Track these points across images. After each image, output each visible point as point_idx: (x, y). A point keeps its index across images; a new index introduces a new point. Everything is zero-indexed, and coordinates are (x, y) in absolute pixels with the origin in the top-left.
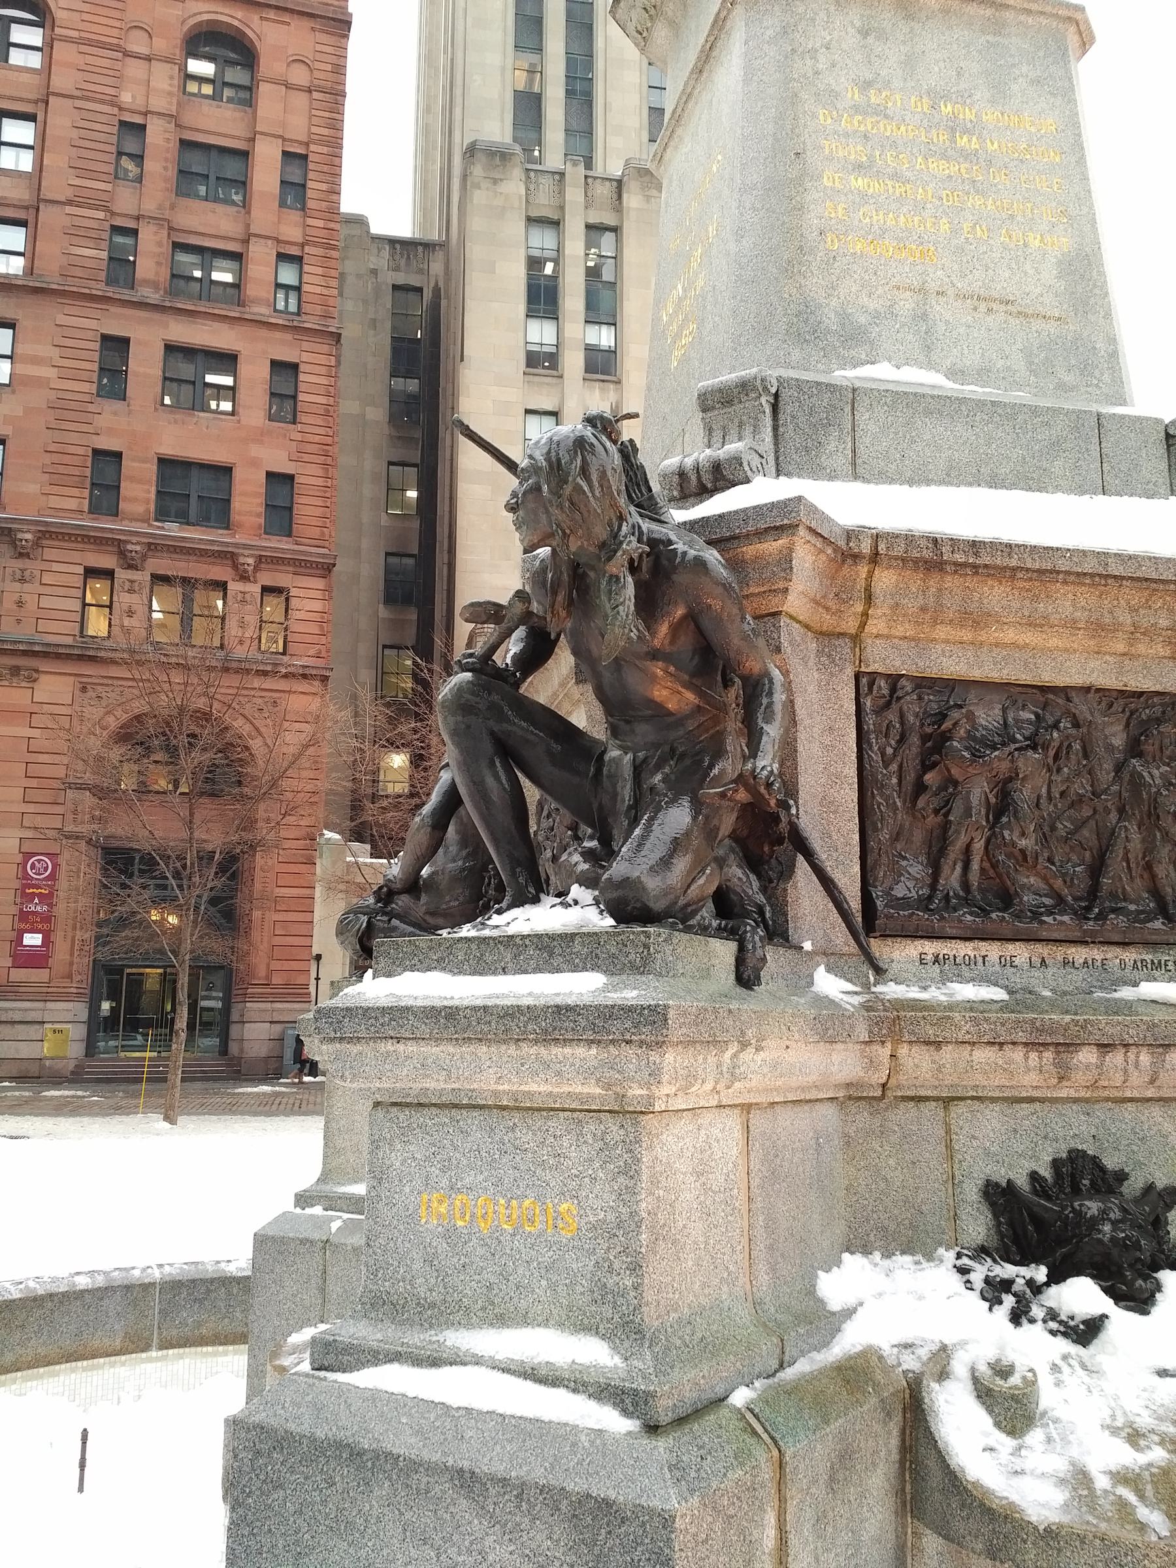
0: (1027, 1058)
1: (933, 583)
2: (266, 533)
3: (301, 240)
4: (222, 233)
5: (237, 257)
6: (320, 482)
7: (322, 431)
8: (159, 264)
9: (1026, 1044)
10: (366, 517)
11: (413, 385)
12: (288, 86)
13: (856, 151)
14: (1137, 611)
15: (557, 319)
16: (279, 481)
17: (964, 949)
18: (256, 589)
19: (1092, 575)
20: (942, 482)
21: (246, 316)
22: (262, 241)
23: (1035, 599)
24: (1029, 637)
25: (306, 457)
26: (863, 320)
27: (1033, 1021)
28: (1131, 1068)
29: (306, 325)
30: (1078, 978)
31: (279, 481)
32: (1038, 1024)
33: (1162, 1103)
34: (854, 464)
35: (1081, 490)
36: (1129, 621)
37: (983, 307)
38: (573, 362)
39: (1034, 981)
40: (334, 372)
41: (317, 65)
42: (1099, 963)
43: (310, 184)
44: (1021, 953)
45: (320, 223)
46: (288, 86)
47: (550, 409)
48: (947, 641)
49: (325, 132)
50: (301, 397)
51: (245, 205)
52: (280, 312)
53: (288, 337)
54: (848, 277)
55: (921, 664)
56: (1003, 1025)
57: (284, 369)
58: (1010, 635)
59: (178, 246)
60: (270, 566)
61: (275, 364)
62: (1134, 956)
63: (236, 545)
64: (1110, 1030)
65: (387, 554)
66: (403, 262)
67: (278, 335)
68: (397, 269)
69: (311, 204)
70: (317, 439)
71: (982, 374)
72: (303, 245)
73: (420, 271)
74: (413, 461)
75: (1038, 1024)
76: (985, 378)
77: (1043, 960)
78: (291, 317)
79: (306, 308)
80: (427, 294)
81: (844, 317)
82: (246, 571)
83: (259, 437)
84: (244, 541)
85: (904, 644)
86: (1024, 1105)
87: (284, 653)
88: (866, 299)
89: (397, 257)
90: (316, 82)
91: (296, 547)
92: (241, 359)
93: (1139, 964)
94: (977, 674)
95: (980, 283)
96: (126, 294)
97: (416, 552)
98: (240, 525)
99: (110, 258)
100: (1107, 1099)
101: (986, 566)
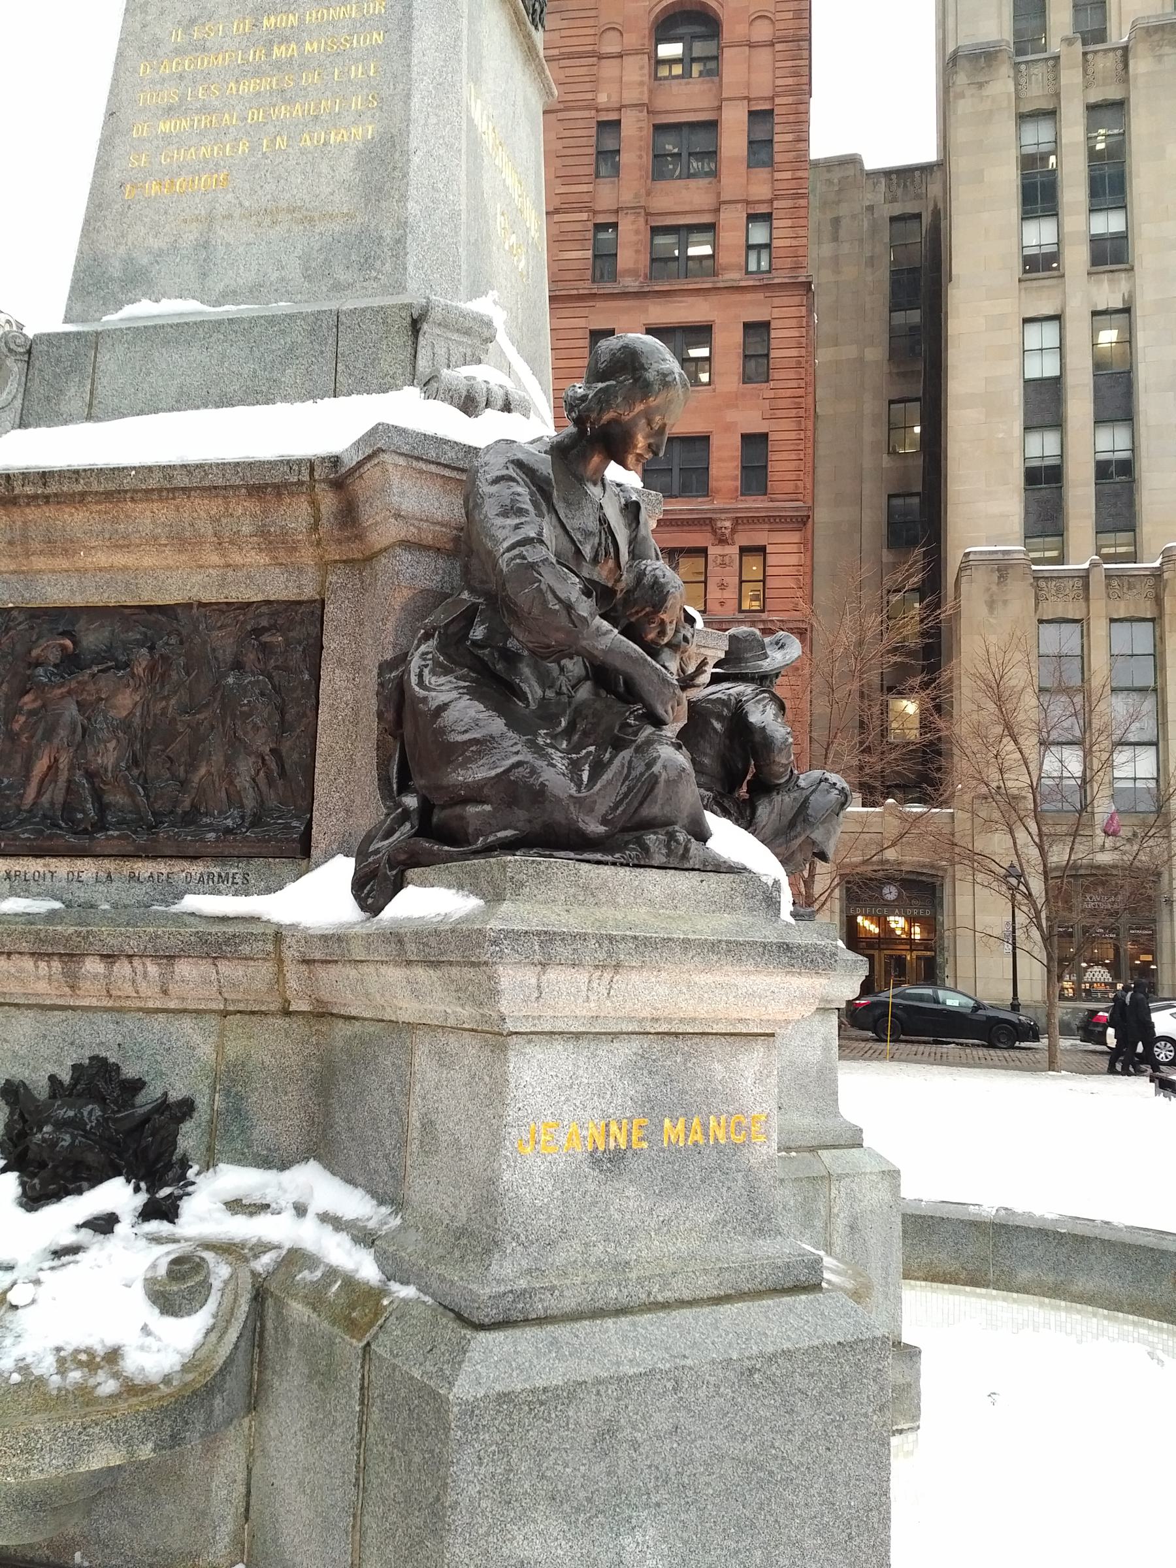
0: (37, 967)
1: (16, 513)
2: (742, 495)
3: (769, 196)
4: (697, 208)
5: (710, 228)
6: (793, 435)
7: (794, 384)
8: (637, 251)
9: (33, 954)
10: (868, 462)
11: (915, 317)
12: (751, 45)
13: (170, 95)
14: (219, 520)
15: (1125, 207)
16: (754, 443)
17: (33, 866)
18: (733, 550)
19: (160, 490)
20: (172, 409)
21: (719, 285)
22: (733, 206)
23: (115, 520)
24: (120, 559)
25: (779, 413)
26: (145, 261)
27: (38, 933)
28: (139, 978)
29: (776, 281)
30: (139, 892)
31: (754, 443)
32: (42, 935)
33: (194, 1015)
34: (90, 405)
35: (312, 395)
36: (210, 532)
37: (267, 221)
38: (1077, 257)
39: (97, 896)
40: (805, 323)
41: (779, 16)
42: (164, 877)
43: (776, 138)
44: (88, 868)
45: (788, 175)
46: (751, 45)
47: (1052, 313)
48: (53, 571)
49: (790, 81)
50: (773, 354)
51: (715, 174)
52: (752, 273)
53: (760, 296)
54: (139, 222)
55: (27, 595)
56: (9, 935)
57: (757, 330)
58: (102, 559)
59: (656, 231)
60: (746, 527)
61: (747, 326)
62: (201, 869)
63: (714, 511)
64: (112, 941)
65: (890, 496)
66: (900, 192)
67: (749, 297)
68: (894, 200)
69: (778, 158)
70: (789, 393)
71: (254, 292)
72: (771, 201)
73: (918, 197)
74: (915, 396)
75: (42, 935)
76: (256, 294)
77: (109, 876)
78: (765, 276)
79: (777, 263)
80: (926, 219)
81: (129, 261)
82: (723, 534)
83: (732, 401)
84: (721, 506)
85: (14, 578)
86: (56, 1013)
87: (763, 611)
88: (151, 240)
89: (894, 188)
90: (779, 34)
91: (771, 504)
92: (715, 329)
93: (206, 878)
94: (78, 601)
95: (269, 197)
96: (609, 288)
97: (919, 489)
98: (718, 491)
99: (595, 256)
100: (140, 1009)
101: (56, 495)
